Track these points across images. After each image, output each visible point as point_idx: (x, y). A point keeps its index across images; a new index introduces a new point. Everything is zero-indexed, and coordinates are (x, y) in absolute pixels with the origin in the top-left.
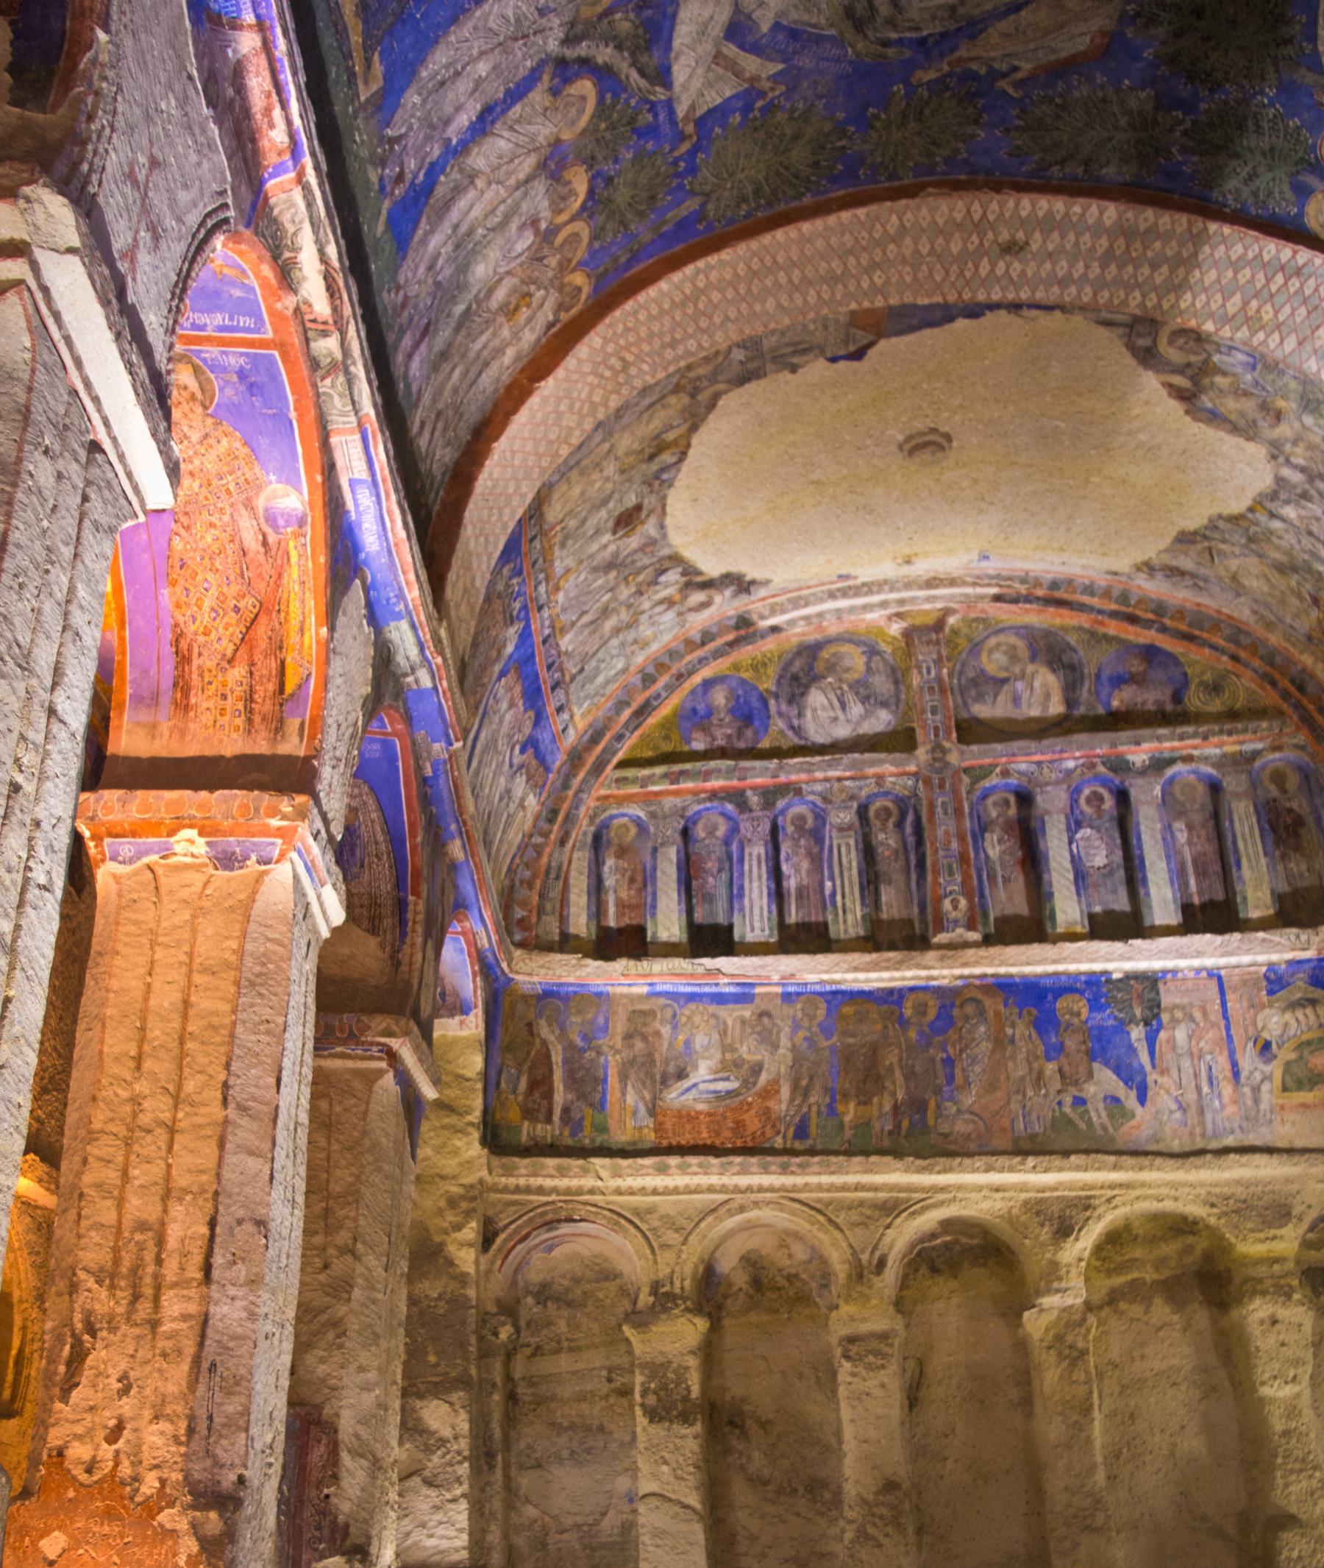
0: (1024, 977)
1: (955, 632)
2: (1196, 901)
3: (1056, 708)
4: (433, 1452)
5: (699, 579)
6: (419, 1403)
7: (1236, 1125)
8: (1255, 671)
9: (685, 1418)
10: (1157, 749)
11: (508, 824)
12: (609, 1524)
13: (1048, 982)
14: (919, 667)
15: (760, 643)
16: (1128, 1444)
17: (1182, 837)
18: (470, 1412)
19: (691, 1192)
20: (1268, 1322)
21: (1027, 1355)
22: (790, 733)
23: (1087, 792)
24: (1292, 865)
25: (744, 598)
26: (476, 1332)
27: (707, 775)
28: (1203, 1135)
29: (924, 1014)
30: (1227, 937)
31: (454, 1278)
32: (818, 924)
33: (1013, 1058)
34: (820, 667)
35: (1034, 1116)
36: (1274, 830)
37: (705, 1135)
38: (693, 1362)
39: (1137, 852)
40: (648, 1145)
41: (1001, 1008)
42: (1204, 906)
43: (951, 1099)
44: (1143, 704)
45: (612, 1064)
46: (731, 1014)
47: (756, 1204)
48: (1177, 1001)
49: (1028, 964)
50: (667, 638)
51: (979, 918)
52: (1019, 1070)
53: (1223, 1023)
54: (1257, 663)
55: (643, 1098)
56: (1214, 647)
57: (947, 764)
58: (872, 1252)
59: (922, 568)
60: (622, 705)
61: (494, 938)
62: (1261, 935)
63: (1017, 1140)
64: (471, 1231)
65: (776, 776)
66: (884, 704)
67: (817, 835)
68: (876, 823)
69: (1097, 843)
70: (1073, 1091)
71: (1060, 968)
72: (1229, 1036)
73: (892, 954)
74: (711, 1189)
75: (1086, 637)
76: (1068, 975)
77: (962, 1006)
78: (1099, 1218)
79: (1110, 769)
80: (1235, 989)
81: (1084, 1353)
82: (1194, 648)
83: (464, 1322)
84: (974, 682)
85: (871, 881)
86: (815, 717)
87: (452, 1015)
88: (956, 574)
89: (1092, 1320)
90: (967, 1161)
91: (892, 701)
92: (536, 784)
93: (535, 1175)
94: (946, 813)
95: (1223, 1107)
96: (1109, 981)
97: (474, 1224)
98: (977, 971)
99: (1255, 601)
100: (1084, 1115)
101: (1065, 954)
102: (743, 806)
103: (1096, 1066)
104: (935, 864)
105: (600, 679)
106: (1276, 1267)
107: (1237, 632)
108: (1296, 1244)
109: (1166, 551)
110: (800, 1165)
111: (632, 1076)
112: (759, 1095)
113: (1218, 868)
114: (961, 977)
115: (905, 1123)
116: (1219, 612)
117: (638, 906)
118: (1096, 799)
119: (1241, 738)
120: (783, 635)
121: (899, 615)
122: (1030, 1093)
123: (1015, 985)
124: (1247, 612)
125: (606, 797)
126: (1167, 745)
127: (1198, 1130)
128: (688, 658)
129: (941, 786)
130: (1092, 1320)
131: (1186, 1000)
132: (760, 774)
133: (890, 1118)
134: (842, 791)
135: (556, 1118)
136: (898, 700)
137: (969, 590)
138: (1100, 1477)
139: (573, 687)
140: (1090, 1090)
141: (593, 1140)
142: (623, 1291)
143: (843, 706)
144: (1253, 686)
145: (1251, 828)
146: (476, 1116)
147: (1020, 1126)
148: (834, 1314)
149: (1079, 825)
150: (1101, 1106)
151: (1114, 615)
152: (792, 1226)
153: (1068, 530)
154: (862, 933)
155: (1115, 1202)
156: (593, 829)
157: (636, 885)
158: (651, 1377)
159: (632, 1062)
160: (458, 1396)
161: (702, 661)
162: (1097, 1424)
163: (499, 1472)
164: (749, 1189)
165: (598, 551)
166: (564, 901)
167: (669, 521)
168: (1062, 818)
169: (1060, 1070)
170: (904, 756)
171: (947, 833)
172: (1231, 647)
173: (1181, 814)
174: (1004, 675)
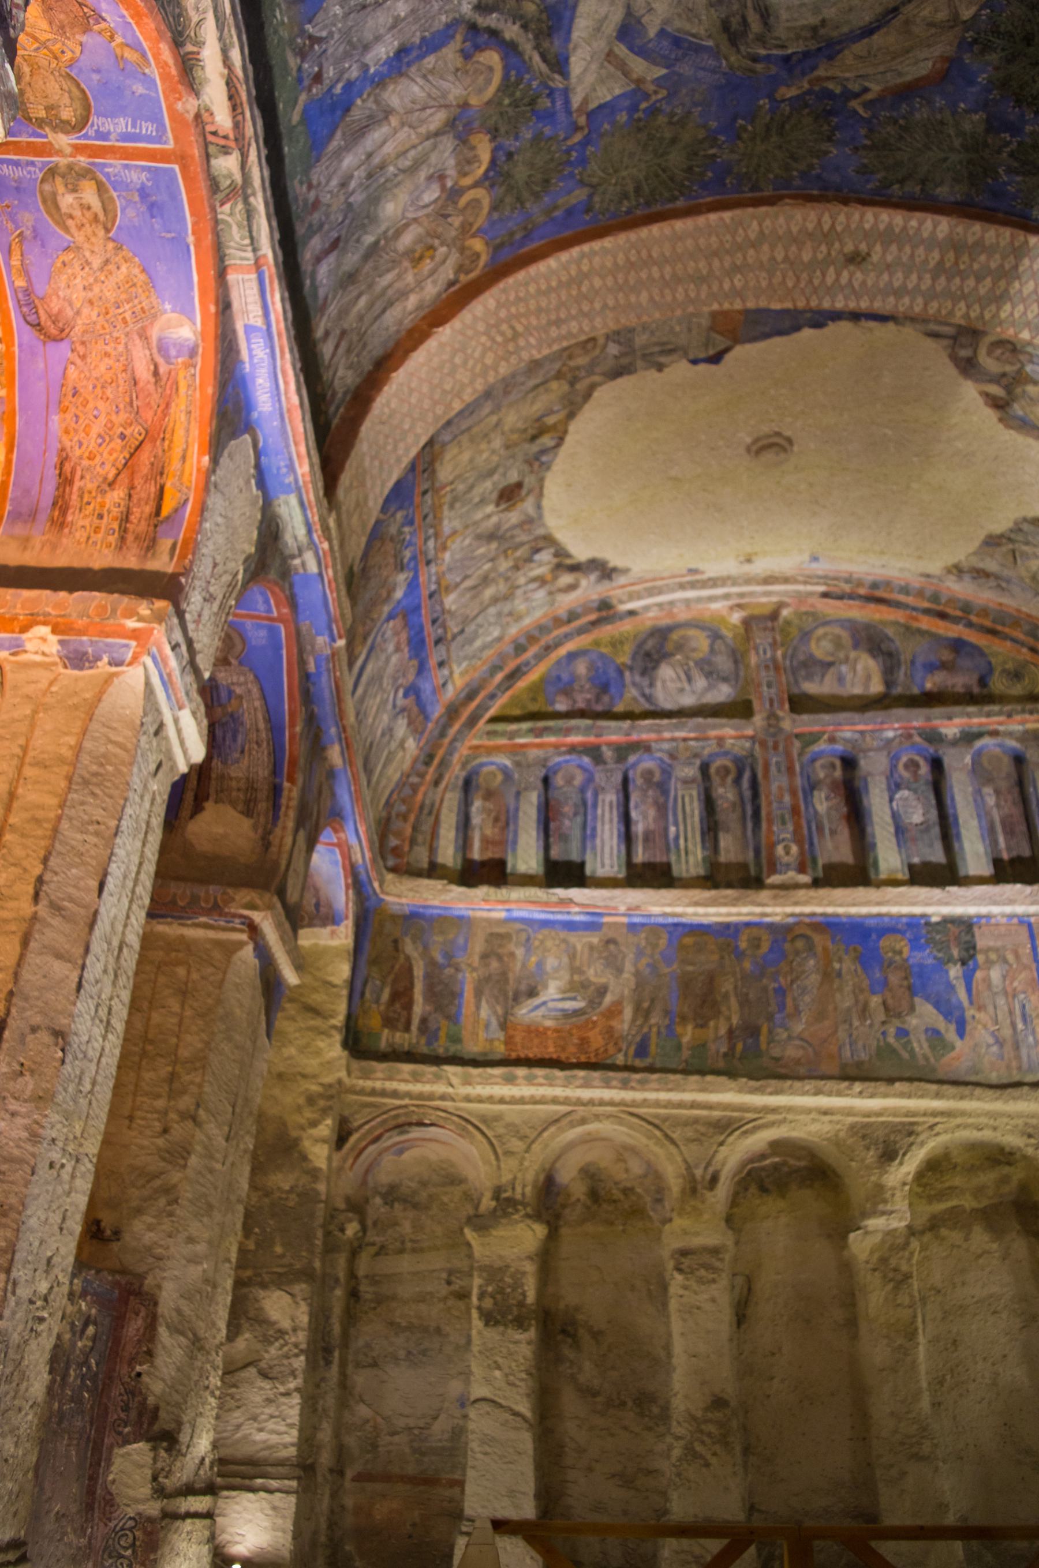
0: (849, 916)
1: (788, 623)
2: (1005, 856)
3: (877, 687)
4: (271, 1343)
5: (568, 562)
6: (262, 1293)
9: (520, 1323)
12: (440, 1429)
13: (872, 922)
14: (756, 648)
15: (619, 623)
16: (952, 1370)
17: (991, 801)
18: (310, 1305)
22: (642, 700)
23: (904, 759)
25: (606, 585)
26: (323, 1226)
27: (568, 731)
28: (1019, 1068)
29: (758, 947)
32: (662, 864)
33: (840, 989)
34: (669, 647)
35: (860, 1044)
37: (551, 1049)
38: (530, 1267)
39: (951, 811)
40: (498, 1057)
42: (1013, 861)
44: (953, 686)
45: (468, 981)
46: (580, 941)
47: (597, 1117)
48: (991, 944)
49: (854, 905)
50: (538, 614)
51: (809, 863)
55: (495, 1012)
56: (1014, 640)
58: (706, 1168)
59: (761, 567)
60: (495, 669)
61: (368, 855)
64: (326, 1128)
65: (628, 734)
66: (725, 680)
67: (663, 788)
68: (716, 780)
69: (914, 803)
70: (897, 1022)
71: (884, 910)
73: (729, 892)
74: (555, 1101)
75: (902, 630)
76: (889, 915)
77: (793, 940)
78: (922, 1144)
81: (908, 1276)
82: (997, 641)
84: (804, 664)
85: (711, 828)
86: (664, 687)
87: (324, 925)
88: (789, 573)
89: (915, 1244)
90: (798, 1084)
92: (416, 729)
94: (779, 771)
97: (329, 1122)
98: (807, 909)
101: (888, 897)
102: (598, 758)
104: (769, 814)
105: (478, 643)
109: (975, 553)
110: (639, 1082)
112: (603, 1014)
113: (1023, 828)
114: (792, 915)
115: (740, 1047)
116: (1019, 611)
118: (913, 765)
120: (638, 618)
121: (740, 606)
122: (856, 1023)
123: (843, 924)
125: (477, 747)
126: (975, 720)
127: (1014, 1064)
129: (775, 747)
130: (915, 1244)
131: (999, 944)
132: (614, 733)
134: (687, 749)
136: (737, 675)
137: (801, 588)
138: (925, 1403)
139: (454, 646)
140: (913, 1022)
141: (447, 1049)
142: (467, 1196)
143: (689, 679)
146: (339, 1020)
147: (847, 1053)
148: (667, 1227)
149: (898, 787)
150: (923, 1037)
151: (927, 612)
152: (632, 1142)
153: (889, 534)
154: (701, 872)
155: (937, 1129)
156: (464, 774)
158: (489, 1281)
159: (487, 979)
160: (301, 1288)
161: (568, 637)
162: (921, 1348)
163: (335, 1368)
164: (591, 1102)
166: (434, 834)
167: (545, 503)
168: (883, 779)
169: (884, 1003)
171: (780, 788)
172: (1030, 641)
173: (989, 780)
174: (830, 659)
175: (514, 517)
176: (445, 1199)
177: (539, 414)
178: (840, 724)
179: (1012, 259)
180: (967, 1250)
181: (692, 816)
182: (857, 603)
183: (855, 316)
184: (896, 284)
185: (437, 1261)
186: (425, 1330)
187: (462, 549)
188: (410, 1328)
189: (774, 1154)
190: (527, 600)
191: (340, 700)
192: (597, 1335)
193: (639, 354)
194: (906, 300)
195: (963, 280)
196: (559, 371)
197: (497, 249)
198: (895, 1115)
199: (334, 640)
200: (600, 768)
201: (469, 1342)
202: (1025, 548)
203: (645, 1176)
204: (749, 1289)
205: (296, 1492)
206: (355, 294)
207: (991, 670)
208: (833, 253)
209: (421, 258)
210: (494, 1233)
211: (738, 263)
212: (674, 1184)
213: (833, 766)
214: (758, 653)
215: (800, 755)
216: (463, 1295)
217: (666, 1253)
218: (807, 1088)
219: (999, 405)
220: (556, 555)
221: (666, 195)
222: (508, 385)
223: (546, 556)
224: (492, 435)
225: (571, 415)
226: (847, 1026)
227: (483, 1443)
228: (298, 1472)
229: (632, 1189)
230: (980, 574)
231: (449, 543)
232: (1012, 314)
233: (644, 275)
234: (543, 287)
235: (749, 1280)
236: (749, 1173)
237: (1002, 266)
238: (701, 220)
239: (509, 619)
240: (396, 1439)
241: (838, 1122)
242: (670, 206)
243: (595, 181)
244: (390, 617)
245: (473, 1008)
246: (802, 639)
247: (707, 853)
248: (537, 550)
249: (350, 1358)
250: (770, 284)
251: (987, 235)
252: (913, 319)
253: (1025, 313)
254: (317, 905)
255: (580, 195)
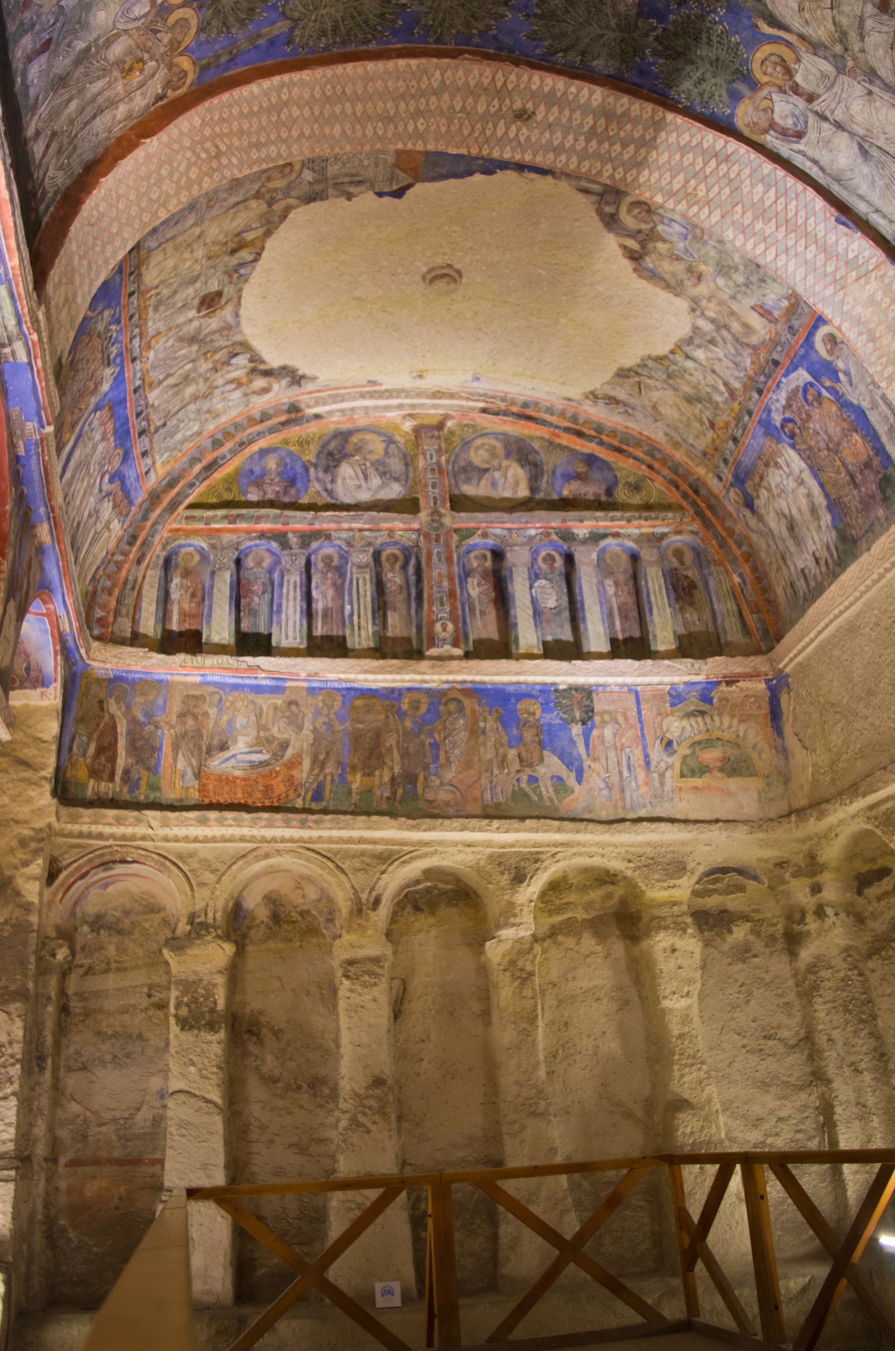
0: (494, 684)
1: (451, 433)
2: (620, 636)
3: (523, 492)
5: (262, 367)
7: (647, 801)
8: (664, 477)
9: (212, 1027)
10: (595, 526)
11: (94, 540)
12: (143, 1118)
13: (512, 689)
14: (424, 454)
15: (305, 425)
17: (611, 590)
18: (25, 1021)
19: (226, 841)
20: (669, 950)
21: (487, 976)
22: (324, 494)
23: (543, 554)
24: (687, 615)
27: (258, 519)
29: (417, 708)
30: (642, 662)
31: (20, 906)
32: (338, 637)
34: (350, 448)
35: (499, 790)
36: (675, 590)
37: (240, 795)
38: (220, 980)
39: (579, 598)
40: (193, 802)
41: (476, 707)
42: (626, 640)
43: (436, 774)
44: (585, 494)
45: (166, 737)
46: (266, 702)
47: (279, 852)
48: (606, 708)
49: (498, 674)
50: (234, 413)
51: (462, 638)
52: (488, 753)
53: (639, 725)
54: (666, 472)
55: (191, 764)
57: (442, 525)
58: (370, 892)
59: (430, 382)
60: (194, 460)
61: (75, 625)
62: (667, 662)
63: (485, 807)
64: (38, 867)
66: (397, 479)
67: (340, 571)
68: (386, 566)
69: (550, 590)
70: (528, 771)
71: (521, 678)
72: (643, 735)
74: (242, 839)
75: (546, 444)
77: (446, 703)
78: (546, 869)
79: (561, 538)
80: (647, 701)
81: (531, 974)
82: (622, 458)
83: (25, 943)
84: (464, 469)
85: (381, 607)
87: (34, 687)
89: (538, 948)
90: (447, 822)
91: (403, 477)
92: (121, 511)
93: (96, 823)
94: (440, 560)
95: (638, 787)
96: (556, 691)
97: (40, 861)
98: (459, 678)
99: (668, 425)
100: (536, 790)
103: (546, 753)
104: (430, 596)
105: (179, 436)
106: (675, 908)
107: (653, 449)
108: (689, 891)
109: (608, 383)
111: (183, 746)
112: (286, 766)
113: (636, 614)
114: (447, 682)
115: (400, 791)
116: (640, 434)
117: (196, 616)
118: (550, 559)
119: (654, 523)
120: (324, 421)
121: (411, 416)
122: (496, 772)
123: (488, 690)
124: (661, 434)
125: (177, 530)
126: (602, 523)
127: (620, 804)
128: (249, 431)
129: (437, 540)
130: (538, 948)
131: (612, 707)
132: (299, 522)
133: (388, 786)
135: (118, 778)
137: (464, 403)
138: (542, 1073)
139: (156, 437)
141: (147, 797)
142: (165, 922)
143: (366, 478)
144: (663, 489)
145: (660, 586)
147: (488, 796)
148: (337, 942)
149: (537, 577)
150: (549, 783)
151: (567, 430)
153: (540, 361)
154: (372, 645)
155: (558, 857)
156: (164, 554)
157: (196, 600)
158: (185, 993)
159: (184, 735)
160: (15, 1007)
162: (540, 1030)
163: (48, 1074)
164: (274, 840)
165: (185, 323)
166: (137, 607)
167: (242, 312)
168: (525, 570)
169: (519, 755)
170: (410, 516)
171: (440, 574)
172: (648, 459)
173: (610, 574)
174: (486, 466)
175: (214, 323)
176: (146, 925)
177: (239, 229)
178: (491, 522)
179: (651, 131)
180: (578, 952)
181: (365, 597)
182: (510, 419)
183: (520, 167)
184: (556, 143)
185: (139, 978)
186: (130, 1036)
187: (165, 349)
188: (116, 1035)
189: (427, 879)
190: (224, 399)
191: (48, 482)
192: (277, 1033)
193: (331, 182)
194: (563, 158)
195: (611, 145)
196: (258, 192)
197: (204, 69)
198: (524, 847)
199: (43, 427)
200: (286, 552)
201: (167, 1045)
202: (648, 381)
203: (319, 900)
204: (405, 989)
205: (15, 1180)
206: (66, 97)
207: (616, 482)
208: (504, 109)
209: (131, 70)
210: (189, 952)
211: (422, 107)
212: (344, 906)
213: (484, 557)
214: (425, 458)
215: (457, 547)
216: (162, 1006)
217: (336, 964)
218: (455, 825)
219: (635, 257)
220: (251, 360)
221: (361, 37)
222: (211, 199)
223: (242, 361)
224: (195, 246)
225: (268, 233)
226: (488, 775)
227: (180, 1126)
228: (16, 1163)
229: (308, 912)
230: (612, 401)
231: (153, 342)
232: (649, 179)
233: (338, 109)
234: (246, 111)
235: (404, 982)
236: (406, 896)
237: (643, 136)
238: (390, 64)
239: (208, 416)
240: (104, 1129)
241: (479, 853)
242: (363, 48)
243: (296, 15)
244: (97, 408)
245: (171, 761)
246: (463, 447)
247: (376, 628)
248: (235, 355)
249: (62, 1064)
250: (448, 131)
251: (633, 108)
252: (568, 176)
253: (659, 180)
254: (28, 669)
255: (282, 27)
